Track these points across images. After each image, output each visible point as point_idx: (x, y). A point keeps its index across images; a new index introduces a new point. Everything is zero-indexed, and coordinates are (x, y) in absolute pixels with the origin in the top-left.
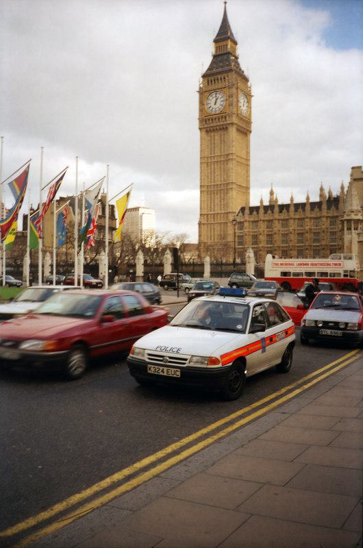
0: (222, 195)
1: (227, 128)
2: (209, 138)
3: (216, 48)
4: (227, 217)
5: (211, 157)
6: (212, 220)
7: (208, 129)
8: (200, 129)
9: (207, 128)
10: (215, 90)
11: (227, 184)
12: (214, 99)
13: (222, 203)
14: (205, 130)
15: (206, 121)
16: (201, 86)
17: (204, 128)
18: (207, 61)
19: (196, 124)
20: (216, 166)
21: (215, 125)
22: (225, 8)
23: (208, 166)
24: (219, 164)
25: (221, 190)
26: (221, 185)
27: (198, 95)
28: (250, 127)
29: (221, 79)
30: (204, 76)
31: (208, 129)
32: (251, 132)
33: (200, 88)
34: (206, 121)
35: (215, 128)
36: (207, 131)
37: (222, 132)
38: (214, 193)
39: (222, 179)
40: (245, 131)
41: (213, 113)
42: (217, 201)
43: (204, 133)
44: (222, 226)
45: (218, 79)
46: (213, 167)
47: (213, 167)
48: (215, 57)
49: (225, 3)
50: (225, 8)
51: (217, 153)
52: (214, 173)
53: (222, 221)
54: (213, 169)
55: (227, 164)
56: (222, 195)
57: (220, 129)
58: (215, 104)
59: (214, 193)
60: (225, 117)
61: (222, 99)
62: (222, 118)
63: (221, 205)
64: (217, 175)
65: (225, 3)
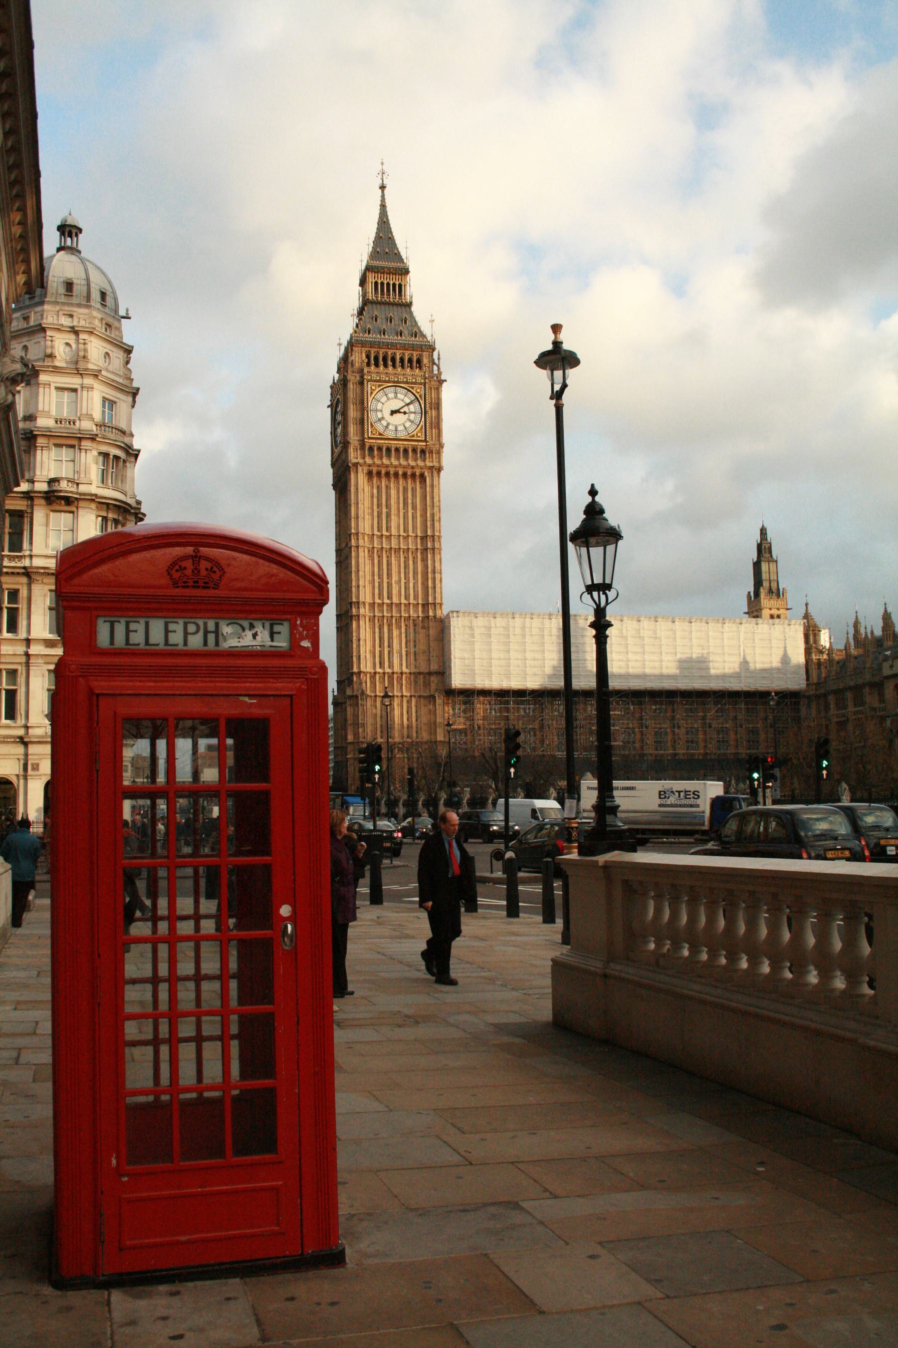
1: (422, 476)
2: (375, 491)
7: (375, 470)
10: (396, 384)
14: (366, 469)
22: (383, 206)
31: (375, 470)
34: (371, 449)
35: (392, 471)
36: (370, 474)
41: (390, 434)
49: (383, 188)
50: (383, 206)
52: (389, 575)
58: (393, 413)
65: (383, 188)
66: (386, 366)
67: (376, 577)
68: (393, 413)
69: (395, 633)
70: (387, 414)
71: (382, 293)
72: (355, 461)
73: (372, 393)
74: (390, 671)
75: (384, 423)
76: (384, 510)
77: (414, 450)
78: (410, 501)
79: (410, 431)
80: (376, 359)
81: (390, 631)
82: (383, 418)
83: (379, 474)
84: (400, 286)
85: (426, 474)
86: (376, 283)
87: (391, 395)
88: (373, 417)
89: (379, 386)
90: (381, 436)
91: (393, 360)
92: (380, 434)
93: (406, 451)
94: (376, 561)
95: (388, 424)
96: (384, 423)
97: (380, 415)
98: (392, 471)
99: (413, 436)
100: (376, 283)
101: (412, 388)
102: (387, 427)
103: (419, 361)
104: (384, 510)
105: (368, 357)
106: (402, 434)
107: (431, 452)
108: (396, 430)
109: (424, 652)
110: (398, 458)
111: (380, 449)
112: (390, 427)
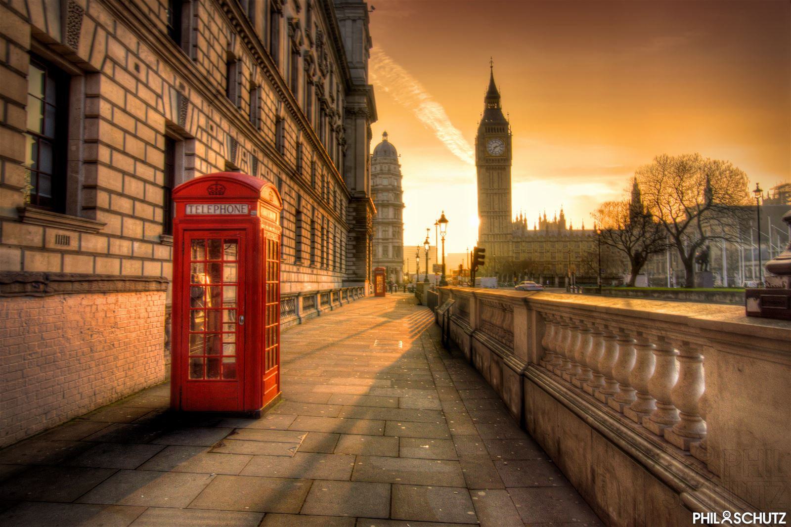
0: (501, 220)
15: (487, 160)
17: (484, 166)
22: (492, 74)
23: (487, 196)
37: (500, 171)
38: (493, 218)
41: (494, 155)
42: (497, 225)
43: (483, 170)
44: (501, 244)
49: (492, 67)
50: (492, 74)
56: (501, 220)
63: (500, 228)
65: (492, 67)
66: (492, 131)
68: (495, 148)
70: (493, 149)
80: (489, 129)
88: (488, 149)
91: (495, 129)
93: (499, 160)
103: (503, 129)
105: (486, 129)
106: (497, 155)
111: (490, 160)
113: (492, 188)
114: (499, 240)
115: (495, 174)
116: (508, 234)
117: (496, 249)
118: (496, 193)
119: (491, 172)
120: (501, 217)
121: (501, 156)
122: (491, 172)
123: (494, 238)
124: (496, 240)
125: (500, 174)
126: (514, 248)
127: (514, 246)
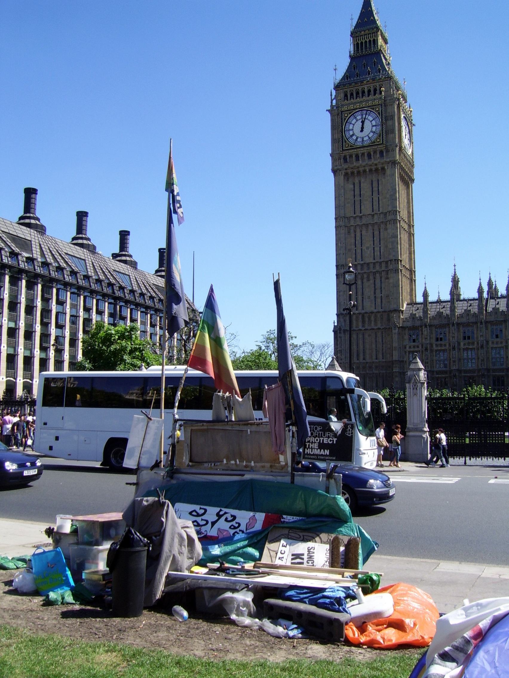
0: (378, 281)
1: (383, 169)
3: (357, 46)
4: (389, 320)
5: (355, 218)
6: (360, 324)
7: (349, 171)
8: (334, 171)
9: (346, 169)
11: (387, 262)
12: (359, 124)
13: (378, 295)
15: (345, 159)
16: (334, 102)
18: (344, 64)
19: (328, 163)
20: (364, 232)
21: (364, 164)
24: (370, 227)
25: (375, 273)
26: (374, 263)
27: (328, 115)
28: (412, 172)
29: (369, 91)
30: (337, 87)
31: (349, 171)
32: (413, 180)
33: (332, 105)
35: (361, 169)
36: (346, 174)
37: (374, 177)
38: (362, 279)
39: (377, 253)
40: (408, 180)
41: (359, 144)
44: (379, 334)
45: (363, 92)
46: (358, 234)
47: (358, 234)
48: (352, 58)
51: (367, 209)
53: (379, 326)
54: (358, 238)
55: (386, 229)
57: (371, 170)
59: (362, 279)
60: (381, 152)
61: (374, 123)
62: (375, 152)
64: (368, 248)
67: (353, 247)
69: (366, 284)
71: (362, 49)
72: (336, 168)
73: (345, 119)
74: (363, 311)
75: (354, 138)
76: (357, 198)
77: (375, 152)
78: (375, 189)
79: (373, 140)
81: (362, 283)
82: (353, 135)
83: (352, 173)
84: (374, 40)
85: (386, 168)
86: (358, 44)
87: (359, 117)
89: (350, 113)
90: (353, 147)
92: (351, 146)
94: (353, 235)
95: (357, 138)
96: (354, 138)
97: (351, 133)
98: (361, 169)
99: (374, 142)
100: (358, 44)
101: (373, 109)
102: (363, 140)
104: (357, 198)
107: (388, 151)
108: (363, 140)
109: (388, 296)
110: (363, 160)
112: (359, 140)
113: (358, 214)
114: (373, 325)
115: (366, 186)
116: (391, 311)
117: (367, 346)
118: (367, 225)
119: (357, 181)
120: (378, 275)
121: (373, 144)
122: (357, 181)
123: (363, 322)
124: (366, 327)
125: (375, 184)
126: (406, 342)
127: (406, 337)
